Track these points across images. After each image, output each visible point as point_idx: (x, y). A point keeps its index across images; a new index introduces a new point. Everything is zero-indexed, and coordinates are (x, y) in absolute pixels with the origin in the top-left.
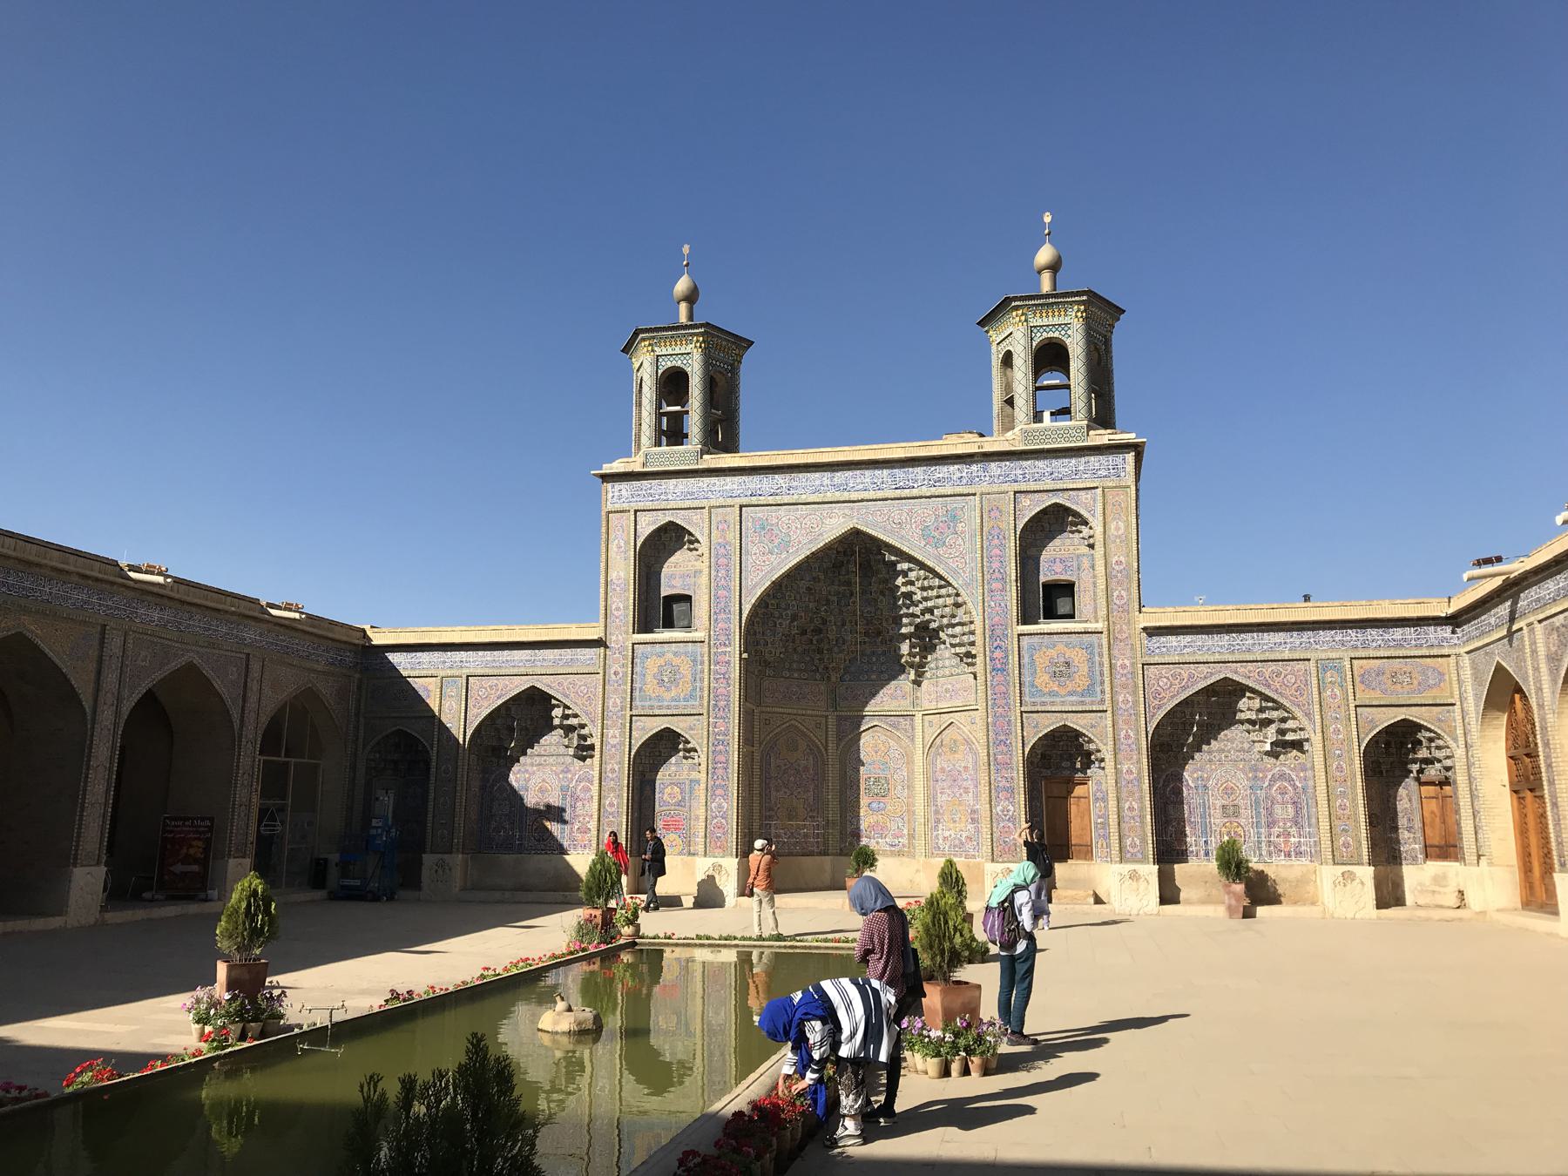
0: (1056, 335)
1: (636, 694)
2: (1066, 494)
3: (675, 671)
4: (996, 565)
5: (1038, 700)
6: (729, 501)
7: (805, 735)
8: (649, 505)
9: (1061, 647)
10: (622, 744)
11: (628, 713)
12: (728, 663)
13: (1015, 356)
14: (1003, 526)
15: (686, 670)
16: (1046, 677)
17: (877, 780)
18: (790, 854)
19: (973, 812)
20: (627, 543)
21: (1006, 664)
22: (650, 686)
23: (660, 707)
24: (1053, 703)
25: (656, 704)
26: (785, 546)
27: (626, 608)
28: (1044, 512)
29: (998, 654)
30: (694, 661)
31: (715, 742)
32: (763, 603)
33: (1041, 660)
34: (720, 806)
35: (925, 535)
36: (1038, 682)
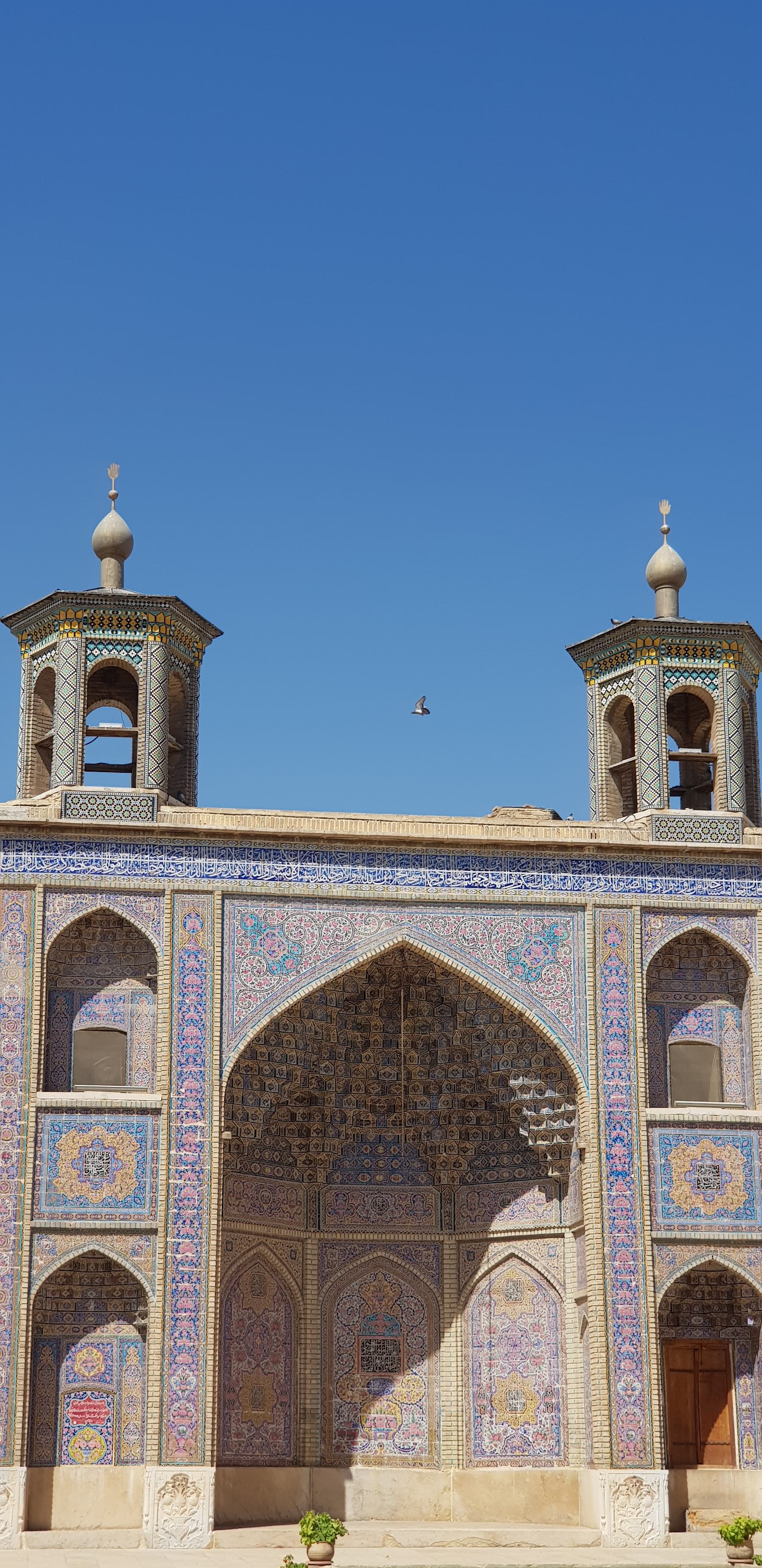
0: (698, 683)
1: (42, 1192)
2: (712, 919)
3: (108, 1156)
4: (614, 1014)
5: (676, 1221)
6: (204, 885)
7: (275, 1271)
8: (71, 881)
9: (706, 1143)
10: (15, 1276)
11: (27, 1224)
12: (200, 1145)
13: (639, 709)
14: (626, 956)
15: (127, 1155)
16: (686, 1188)
17: (381, 1345)
18: (255, 1464)
19: (550, 1393)
20: (28, 938)
21: (631, 1164)
22: (67, 1180)
23: (82, 1217)
24: (695, 1228)
25: (76, 1210)
26: (293, 962)
27: (25, 1047)
28: (677, 940)
29: (618, 1149)
30: (142, 1141)
31: (177, 1276)
32: (251, 1052)
33: (679, 1162)
34: (184, 1381)
35: (512, 960)
36: (675, 1194)
